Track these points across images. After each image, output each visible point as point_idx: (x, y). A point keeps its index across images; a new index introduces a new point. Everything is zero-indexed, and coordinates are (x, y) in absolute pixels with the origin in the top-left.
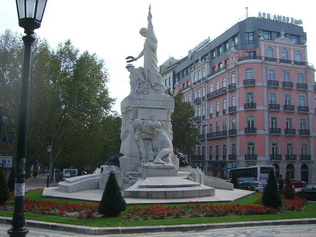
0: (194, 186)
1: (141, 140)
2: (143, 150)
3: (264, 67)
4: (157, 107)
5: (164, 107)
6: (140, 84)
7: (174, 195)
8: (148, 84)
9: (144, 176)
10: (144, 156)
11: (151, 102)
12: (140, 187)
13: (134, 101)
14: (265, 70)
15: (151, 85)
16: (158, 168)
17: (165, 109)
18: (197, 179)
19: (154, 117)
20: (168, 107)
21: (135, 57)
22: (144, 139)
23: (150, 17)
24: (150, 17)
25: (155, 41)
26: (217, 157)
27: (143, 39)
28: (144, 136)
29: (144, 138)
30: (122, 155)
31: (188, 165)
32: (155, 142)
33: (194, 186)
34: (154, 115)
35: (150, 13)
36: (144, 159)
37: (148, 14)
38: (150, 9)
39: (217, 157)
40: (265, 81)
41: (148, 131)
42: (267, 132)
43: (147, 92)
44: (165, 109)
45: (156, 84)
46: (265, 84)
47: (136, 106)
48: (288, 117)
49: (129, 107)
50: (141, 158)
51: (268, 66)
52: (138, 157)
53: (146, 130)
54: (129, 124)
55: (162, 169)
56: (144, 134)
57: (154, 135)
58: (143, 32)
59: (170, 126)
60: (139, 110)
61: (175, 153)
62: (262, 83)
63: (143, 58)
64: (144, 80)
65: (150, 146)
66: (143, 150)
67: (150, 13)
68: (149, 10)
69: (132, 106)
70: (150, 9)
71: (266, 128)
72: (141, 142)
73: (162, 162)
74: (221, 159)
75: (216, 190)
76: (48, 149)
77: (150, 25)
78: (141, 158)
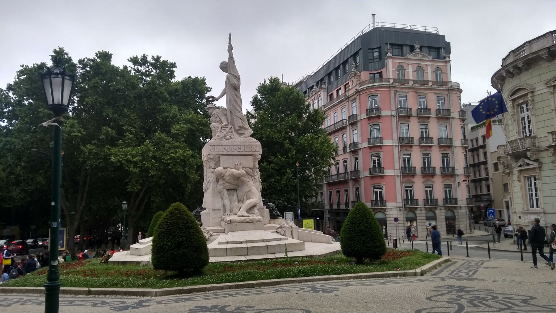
0: (281, 239)
2: (227, 202)
3: (392, 92)
4: (242, 153)
5: (250, 153)
7: (258, 250)
9: (226, 231)
10: (228, 208)
11: (235, 148)
12: (220, 243)
14: (393, 95)
15: (234, 128)
16: (242, 222)
17: (251, 155)
18: (288, 233)
20: (254, 153)
21: (216, 96)
22: (228, 190)
23: (230, 49)
25: (238, 78)
26: (339, 204)
27: (224, 76)
29: (228, 188)
30: (205, 209)
31: (279, 216)
33: (281, 239)
35: (230, 43)
36: (228, 212)
38: (230, 39)
39: (339, 204)
40: (393, 108)
41: (231, 181)
42: (398, 173)
44: (251, 155)
45: (240, 127)
46: (394, 113)
47: (217, 153)
48: (425, 152)
49: (209, 155)
50: (225, 211)
51: (399, 90)
52: (222, 209)
54: (210, 174)
55: (247, 222)
56: (227, 184)
58: (224, 67)
59: (258, 174)
61: (265, 203)
62: (390, 111)
63: (224, 97)
64: (226, 123)
65: (235, 197)
66: (227, 202)
67: (230, 43)
69: (214, 153)
70: (230, 39)
71: (397, 166)
72: (225, 192)
73: (246, 214)
74: (343, 206)
75: (305, 243)
76: (123, 205)
77: (231, 57)
78: (225, 211)
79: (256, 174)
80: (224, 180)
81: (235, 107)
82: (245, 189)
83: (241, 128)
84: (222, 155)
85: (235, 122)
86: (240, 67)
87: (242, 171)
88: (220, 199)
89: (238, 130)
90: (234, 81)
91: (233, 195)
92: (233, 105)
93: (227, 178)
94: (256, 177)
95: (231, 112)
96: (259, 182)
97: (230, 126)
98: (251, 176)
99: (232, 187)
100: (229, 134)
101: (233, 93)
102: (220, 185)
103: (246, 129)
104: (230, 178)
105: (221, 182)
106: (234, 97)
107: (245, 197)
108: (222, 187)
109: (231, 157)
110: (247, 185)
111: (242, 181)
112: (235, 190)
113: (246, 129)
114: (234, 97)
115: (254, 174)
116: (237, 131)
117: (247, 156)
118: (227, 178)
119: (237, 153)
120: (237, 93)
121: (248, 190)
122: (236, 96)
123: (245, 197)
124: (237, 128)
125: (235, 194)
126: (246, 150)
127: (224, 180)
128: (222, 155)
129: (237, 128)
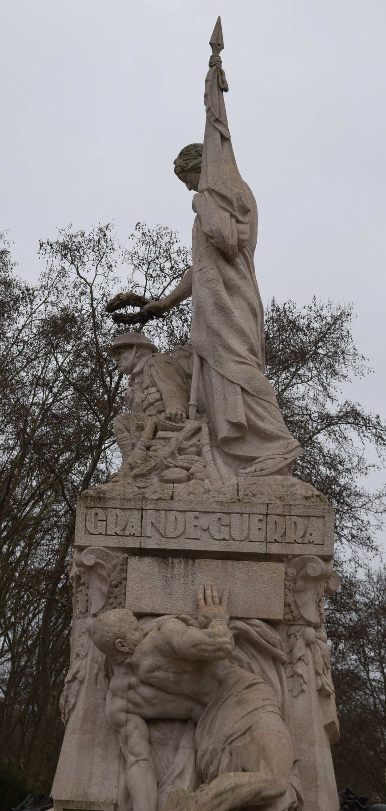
1: (136, 721)
5: (275, 549)
6: (156, 431)
8: (199, 430)
11: (204, 521)
13: (111, 519)
15: (213, 434)
17: (278, 558)
19: (209, 599)
20: (296, 550)
22: (151, 722)
23: (217, 83)
24: (217, 83)
25: (241, 207)
28: (147, 700)
29: (150, 712)
32: (206, 744)
34: (208, 592)
35: (215, 63)
37: (204, 70)
38: (217, 44)
43: (188, 469)
44: (278, 558)
45: (237, 426)
47: (114, 542)
53: (158, 668)
54: (85, 639)
56: (146, 691)
57: (207, 699)
60: (134, 562)
66: (140, 777)
67: (215, 63)
68: (209, 52)
70: (217, 44)
79: (300, 650)
80: (133, 668)
81: (216, 334)
82: (228, 720)
83: (244, 431)
84: (141, 553)
85: (218, 402)
86: (253, 162)
87: (221, 632)
88: (115, 765)
89: (227, 441)
90: (222, 222)
91: (176, 748)
92: (209, 327)
93: (146, 663)
94: (300, 668)
95: (202, 360)
96: (322, 692)
97: (190, 425)
98: (276, 660)
99: (176, 707)
100: (182, 460)
101: (213, 273)
102: (114, 695)
103: (267, 437)
104: (160, 660)
105: (120, 680)
106: (215, 294)
107: (225, 760)
108: (121, 703)
109: (179, 565)
110: (239, 703)
111: (221, 683)
112: (187, 721)
113: (267, 437)
114: (215, 294)
115: (291, 652)
116: (221, 445)
117: (256, 566)
118: (146, 663)
119: (216, 547)
120: (231, 273)
121: (242, 725)
122: (229, 287)
123: (225, 760)
124: (224, 431)
125: (185, 742)
126: (255, 535)
127: (133, 668)
128: (141, 553)
129: (224, 431)
